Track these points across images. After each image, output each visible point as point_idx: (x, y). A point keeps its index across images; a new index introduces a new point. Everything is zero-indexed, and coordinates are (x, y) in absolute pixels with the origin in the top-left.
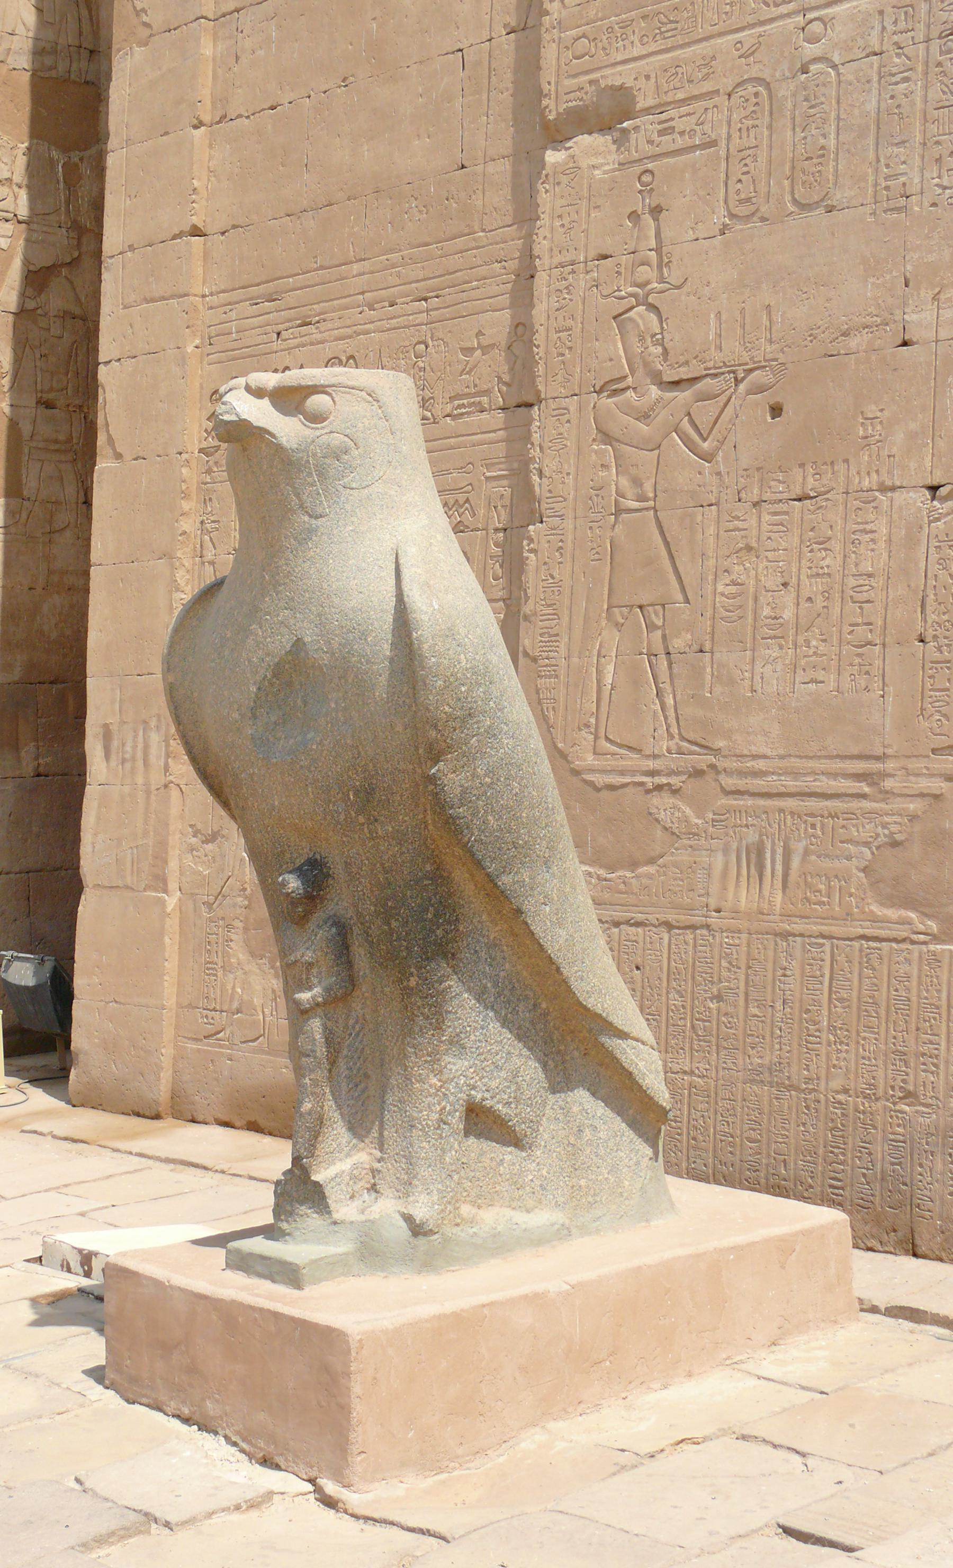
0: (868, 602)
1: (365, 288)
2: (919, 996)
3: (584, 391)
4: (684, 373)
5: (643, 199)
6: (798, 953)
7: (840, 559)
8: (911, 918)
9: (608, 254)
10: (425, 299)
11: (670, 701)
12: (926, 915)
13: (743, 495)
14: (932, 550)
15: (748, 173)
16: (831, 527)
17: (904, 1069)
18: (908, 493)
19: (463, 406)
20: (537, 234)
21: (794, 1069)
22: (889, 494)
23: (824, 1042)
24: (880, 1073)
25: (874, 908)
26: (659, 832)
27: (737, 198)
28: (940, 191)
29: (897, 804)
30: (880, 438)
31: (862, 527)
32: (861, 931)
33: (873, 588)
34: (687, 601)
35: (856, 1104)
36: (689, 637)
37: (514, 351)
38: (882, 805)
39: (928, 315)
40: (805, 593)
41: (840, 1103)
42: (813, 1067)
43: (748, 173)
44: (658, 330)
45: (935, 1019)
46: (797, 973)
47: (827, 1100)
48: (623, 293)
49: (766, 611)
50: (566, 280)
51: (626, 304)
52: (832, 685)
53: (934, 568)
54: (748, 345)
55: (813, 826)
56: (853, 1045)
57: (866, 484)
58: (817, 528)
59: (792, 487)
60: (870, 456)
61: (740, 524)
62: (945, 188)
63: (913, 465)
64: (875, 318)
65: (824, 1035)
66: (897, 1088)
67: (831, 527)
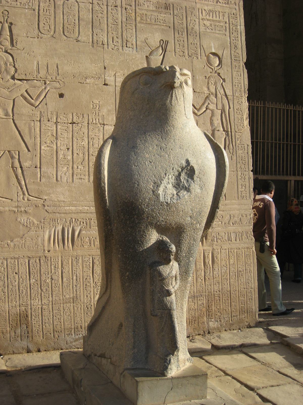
7: (87, 142)
11: (23, 183)
16: (84, 133)
18: (109, 126)
26: (21, 227)
28: (114, 46)
31: (94, 134)
34: (29, 151)
36: (31, 162)
40: (75, 152)
42: (89, 296)
46: (81, 267)
58: (78, 133)
59: (69, 119)
63: (110, 119)
65: (92, 285)
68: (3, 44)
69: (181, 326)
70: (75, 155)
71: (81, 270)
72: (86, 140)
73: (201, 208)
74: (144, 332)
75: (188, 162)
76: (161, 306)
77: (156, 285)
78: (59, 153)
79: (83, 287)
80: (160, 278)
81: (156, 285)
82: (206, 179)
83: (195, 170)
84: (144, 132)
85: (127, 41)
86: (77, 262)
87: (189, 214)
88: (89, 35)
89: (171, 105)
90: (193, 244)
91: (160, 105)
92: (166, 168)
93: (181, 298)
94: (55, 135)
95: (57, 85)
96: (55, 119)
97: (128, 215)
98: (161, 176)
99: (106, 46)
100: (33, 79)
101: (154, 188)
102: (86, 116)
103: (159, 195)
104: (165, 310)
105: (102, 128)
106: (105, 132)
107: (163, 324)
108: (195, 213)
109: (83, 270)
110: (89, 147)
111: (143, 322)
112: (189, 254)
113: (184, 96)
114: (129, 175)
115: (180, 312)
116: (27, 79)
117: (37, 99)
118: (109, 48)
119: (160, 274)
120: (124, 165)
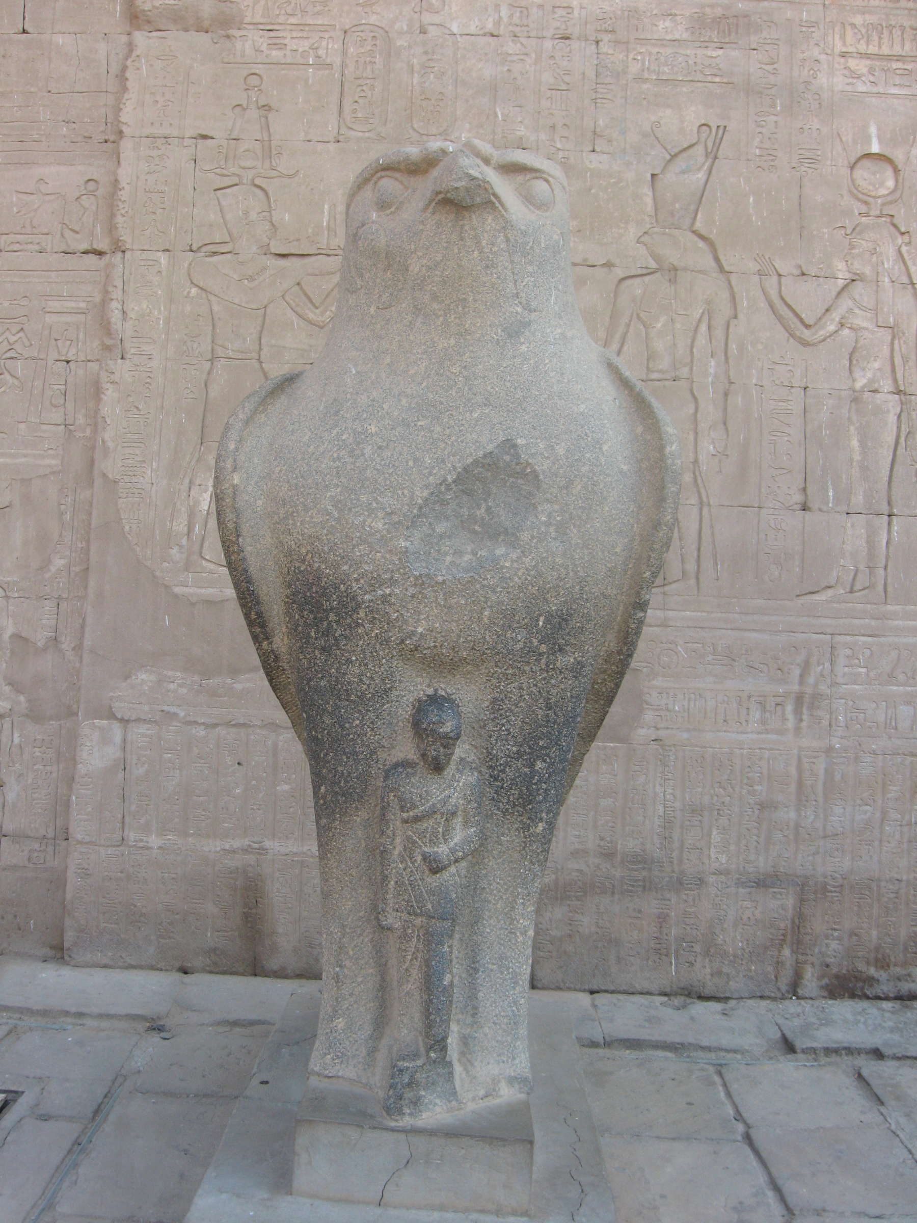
9: (210, 134)
37: (83, 203)
69: (502, 973)
73: (566, 602)
74: (371, 970)
75: (509, 445)
76: (404, 900)
80: (405, 815)
83: (541, 477)
84: (374, 357)
89: (459, 266)
91: (424, 268)
92: (433, 467)
97: (311, 612)
101: (389, 532)
104: (416, 915)
107: (409, 957)
108: (542, 619)
111: (372, 941)
112: (530, 748)
114: (311, 488)
120: (300, 457)
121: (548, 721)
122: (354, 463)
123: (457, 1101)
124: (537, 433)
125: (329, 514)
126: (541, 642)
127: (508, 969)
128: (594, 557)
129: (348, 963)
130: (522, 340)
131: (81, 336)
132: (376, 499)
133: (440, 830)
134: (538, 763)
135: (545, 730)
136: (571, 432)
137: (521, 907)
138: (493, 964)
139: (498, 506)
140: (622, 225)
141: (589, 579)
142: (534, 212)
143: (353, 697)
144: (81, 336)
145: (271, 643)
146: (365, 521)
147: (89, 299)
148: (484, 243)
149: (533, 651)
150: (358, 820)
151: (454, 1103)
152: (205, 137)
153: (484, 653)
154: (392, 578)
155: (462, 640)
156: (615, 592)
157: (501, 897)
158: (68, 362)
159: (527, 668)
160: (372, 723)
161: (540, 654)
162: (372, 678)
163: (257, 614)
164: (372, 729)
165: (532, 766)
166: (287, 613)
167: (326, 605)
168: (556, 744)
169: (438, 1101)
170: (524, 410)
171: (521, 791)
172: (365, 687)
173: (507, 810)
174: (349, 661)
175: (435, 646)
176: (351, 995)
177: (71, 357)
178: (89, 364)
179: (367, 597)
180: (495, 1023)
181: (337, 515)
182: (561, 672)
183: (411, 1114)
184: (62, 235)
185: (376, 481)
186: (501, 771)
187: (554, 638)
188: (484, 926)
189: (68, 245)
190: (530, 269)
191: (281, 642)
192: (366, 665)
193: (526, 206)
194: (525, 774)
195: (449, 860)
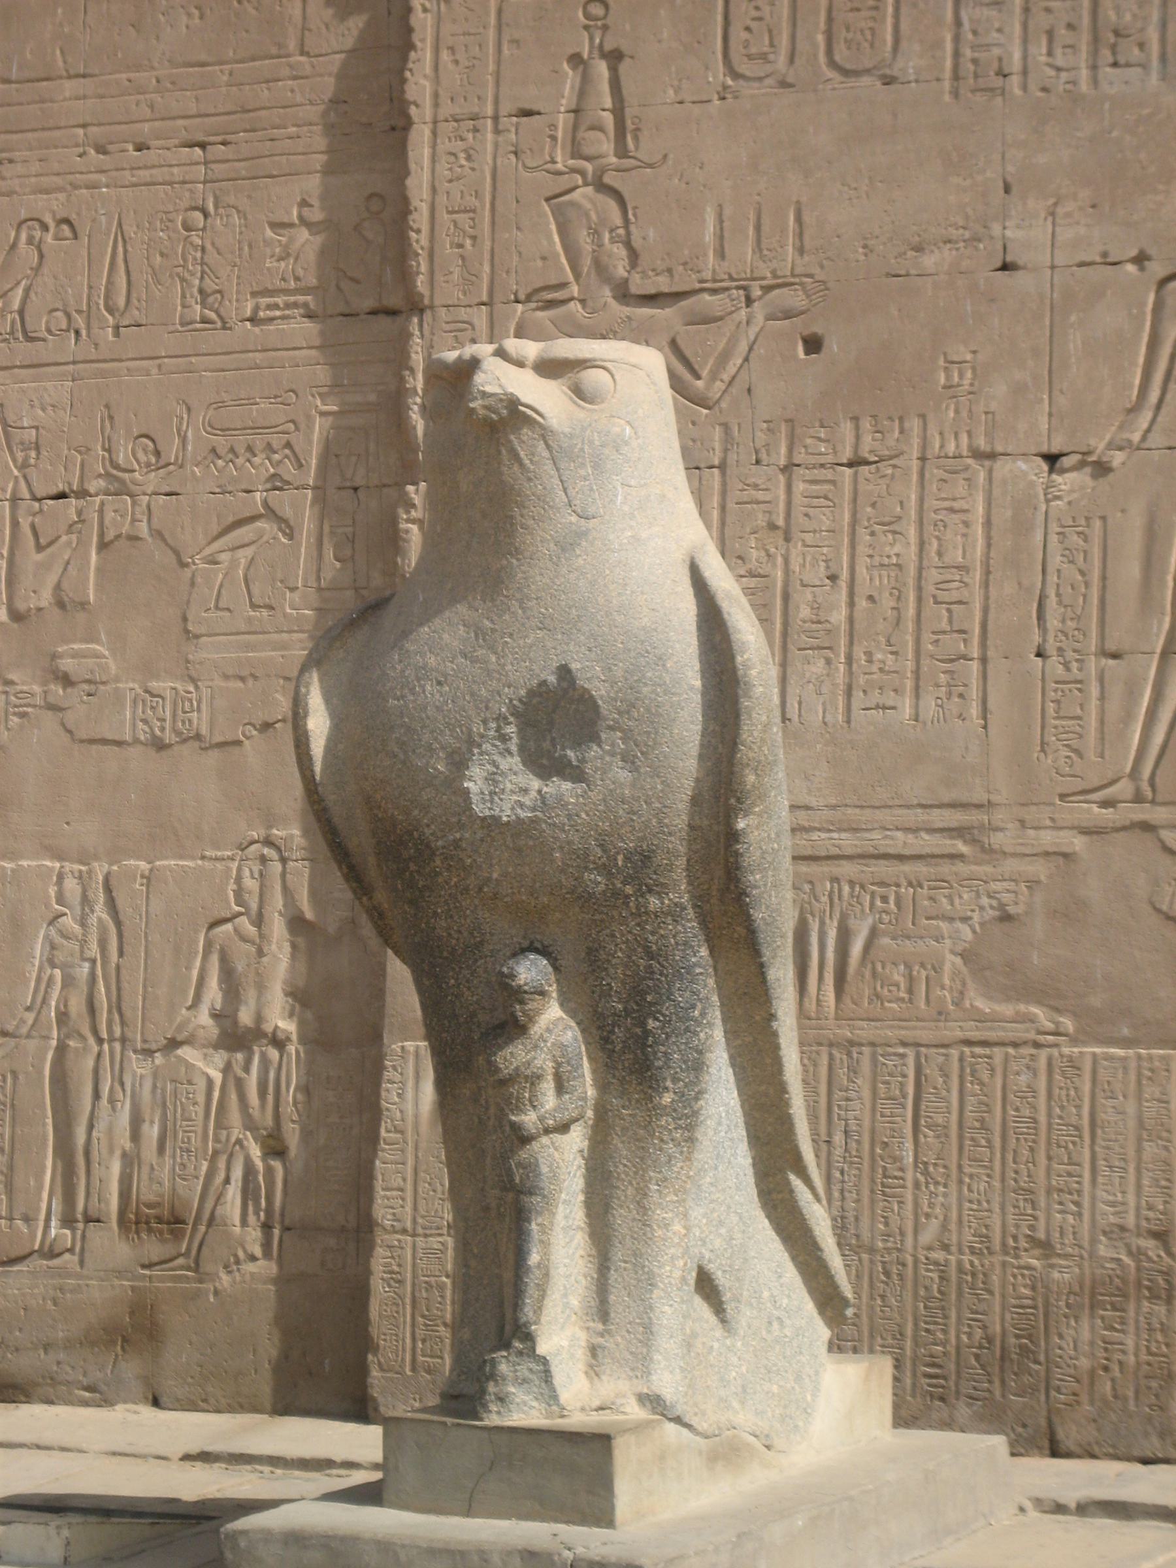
0: (960, 602)
1: (88, 119)
2: (1049, 1115)
3: (499, 297)
4: (663, 284)
5: (591, 39)
6: (866, 1066)
7: (914, 549)
8: (1035, 1015)
9: (535, 107)
10: (203, 146)
12: (1057, 1010)
13: (763, 456)
14: (1053, 539)
15: (760, 19)
16: (901, 503)
17: (1030, 1212)
18: (1014, 462)
19: (276, 306)
20: (411, 70)
21: (865, 1222)
22: (987, 463)
23: (909, 1184)
24: (996, 1222)
25: (982, 1004)
27: (744, 51)
28: (1053, 73)
29: (1011, 866)
30: (971, 389)
31: (947, 504)
32: (959, 1034)
33: (966, 585)
35: (960, 1263)
38: (988, 869)
39: (1040, 232)
40: (862, 590)
41: (936, 1263)
42: (895, 1221)
43: (760, 19)
44: (618, 221)
45: (1074, 1143)
46: (866, 1094)
47: (916, 1261)
48: (560, 166)
49: (805, 612)
50: (462, 139)
51: (565, 182)
52: (907, 711)
53: (1056, 560)
54: (765, 252)
55: (885, 899)
56: (953, 1186)
57: (951, 448)
58: (878, 505)
59: (839, 448)
60: (957, 411)
61: (760, 495)
62: (1059, 69)
64: (961, 231)
65: (909, 1176)
66: (1021, 1237)
67: (901, 503)
68: (587, 150)
69: (636, 1273)
70: (862, 603)
71: (868, 1105)
72: (912, 532)
75: (564, 672)
77: (487, 1102)
78: (795, 597)
79: (873, 1181)
81: (487, 1102)
82: (648, 733)
83: (600, 702)
85: (1117, 33)
86: (854, 1070)
87: (592, 858)
88: (938, 44)
90: (650, 970)
92: (489, 701)
93: (634, 1166)
94: (781, 522)
95: (794, 299)
96: (783, 450)
98: (470, 730)
99: (1015, 80)
100: (698, 286)
102: (914, 424)
103: (467, 792)
105: (982, 476)
106: (996, 492)
108: (620, 858)
109: (874, 1110)
110: (925, 563)
112: (637, 1004)
113: (550, 442)
115: (634, 1219)
116: (675, 289)
117: (714, 376)
118: (1033, 87)
119: (493, 1068)
121: (653, 973)
122: (414, 701)
123: (558, 1405)
124: (593, 656)
125: (395, 756)
126: (625, 883)
127: (644, 1266)
128: (668, 786)
129: (473, 1263)
130: (578, 552)
131: (372, 447)
132: (436, 739)
133: (527, 1095)
134: (650, 1021)
135: (650, 983)
136: (629, 650)
137: (656, 1195)
138: (625, 1262)
139: (563, 736)
140: (1161, 187)
141: (665, 810)
142: (583, 408)
143: (445, 954)
144: (372, 447)
145: (371, 898)
146: (428, 762)
147: (380, 388)
148: (522, 454)
149: (616, 894)
150: (468, 1093)
151: (554, 1408)
152: (528, 113)
153: (565, 899)
154: (460, 821)
155: (538, 884)
156: (706, 822)
157: (630, 1183)
158: (356, 489)
159: (615, 913)
160: (468, 981)
161: (627, 897)
162: (460, 932)
163: (348, 867)
164: (469, 989)
165: (643, 1024)
166: (379, 865)
167: (405, 854)
168: (668, 998)
169: (535, 1404)
170: (579, 630)
171: (636, 1054)
172: (454, 942)
173: (624, 1077)
174: (435, 913)
175: (513, 893)
176: (477, 1300)
177: (359, 481)
178: (385, 490)
179: (440, 843)
180: (628, 1332)
181: (402, 756)
182: (657, 916)
183: (499, 1413)
184: (338, 287)
185: (436, 719)
186: (609, 1032)
187: (638, 878)
188: (613, 1216)
189: (347, 302)
190: (582, 472)
191: (381, 896)
192: (451, 917)
193: (575, 403)
194: (636, 1034)
195: (537, 1128)
